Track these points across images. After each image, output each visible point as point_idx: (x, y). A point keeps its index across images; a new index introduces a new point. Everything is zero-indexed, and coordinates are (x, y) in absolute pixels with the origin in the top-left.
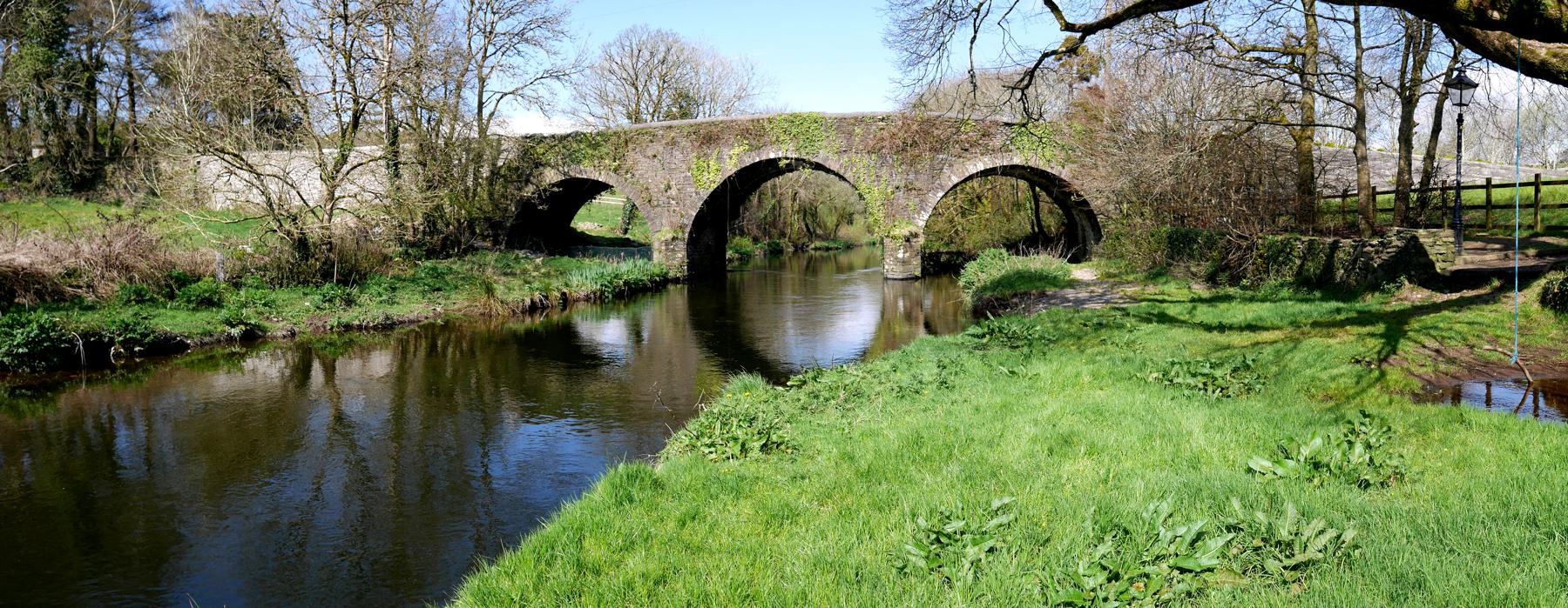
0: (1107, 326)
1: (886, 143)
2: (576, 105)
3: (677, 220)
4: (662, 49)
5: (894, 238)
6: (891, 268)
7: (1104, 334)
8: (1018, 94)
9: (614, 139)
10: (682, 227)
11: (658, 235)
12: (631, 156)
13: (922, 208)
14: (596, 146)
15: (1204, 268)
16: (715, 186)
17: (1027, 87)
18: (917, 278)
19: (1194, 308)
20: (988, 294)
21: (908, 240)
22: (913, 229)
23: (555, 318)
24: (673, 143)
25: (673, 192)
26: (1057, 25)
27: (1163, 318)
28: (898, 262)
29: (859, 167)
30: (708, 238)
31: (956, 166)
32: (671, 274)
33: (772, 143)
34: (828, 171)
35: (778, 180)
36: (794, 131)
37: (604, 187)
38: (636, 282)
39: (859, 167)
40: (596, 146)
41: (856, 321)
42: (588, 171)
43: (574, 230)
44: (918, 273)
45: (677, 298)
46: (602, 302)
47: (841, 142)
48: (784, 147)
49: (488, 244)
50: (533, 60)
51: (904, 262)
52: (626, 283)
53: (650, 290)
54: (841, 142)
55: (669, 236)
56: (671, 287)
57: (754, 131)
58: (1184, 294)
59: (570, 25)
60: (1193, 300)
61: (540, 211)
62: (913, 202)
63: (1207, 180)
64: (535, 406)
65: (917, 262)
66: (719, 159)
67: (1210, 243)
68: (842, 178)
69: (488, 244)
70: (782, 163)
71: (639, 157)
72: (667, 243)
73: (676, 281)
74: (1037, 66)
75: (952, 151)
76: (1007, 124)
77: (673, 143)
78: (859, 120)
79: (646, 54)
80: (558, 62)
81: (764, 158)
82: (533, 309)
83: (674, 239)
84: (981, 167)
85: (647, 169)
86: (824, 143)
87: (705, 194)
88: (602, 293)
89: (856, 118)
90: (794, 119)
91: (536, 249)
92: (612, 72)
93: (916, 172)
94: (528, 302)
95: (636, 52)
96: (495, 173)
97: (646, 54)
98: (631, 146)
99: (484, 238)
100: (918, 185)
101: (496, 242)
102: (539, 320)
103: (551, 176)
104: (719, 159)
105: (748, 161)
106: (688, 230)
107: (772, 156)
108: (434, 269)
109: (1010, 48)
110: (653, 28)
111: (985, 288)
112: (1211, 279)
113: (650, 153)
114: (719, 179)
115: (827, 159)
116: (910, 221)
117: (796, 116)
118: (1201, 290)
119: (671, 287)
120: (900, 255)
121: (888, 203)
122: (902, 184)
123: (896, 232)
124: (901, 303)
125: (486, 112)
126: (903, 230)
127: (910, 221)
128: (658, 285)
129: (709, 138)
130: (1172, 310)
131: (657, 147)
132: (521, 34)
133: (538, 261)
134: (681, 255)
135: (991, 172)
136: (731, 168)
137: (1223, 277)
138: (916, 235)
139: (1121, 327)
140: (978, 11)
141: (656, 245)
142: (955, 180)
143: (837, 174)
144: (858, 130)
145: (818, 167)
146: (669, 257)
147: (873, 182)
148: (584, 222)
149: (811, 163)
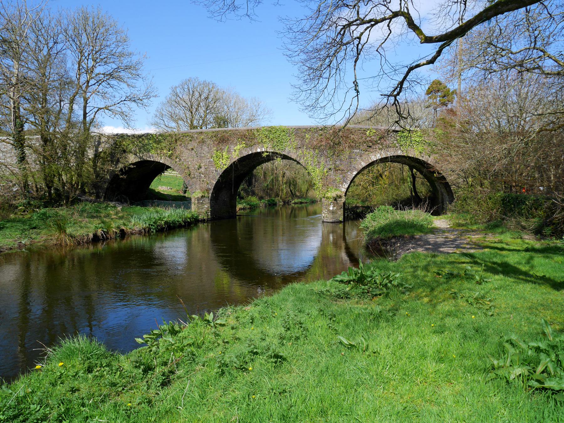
0: (458, 276)
1: (324, 143)
2: (157, 120)
3: (204, 186)
4: (206, 91)
5: (328, 198)
6: (325, 215)
7: (455, 284)
8: (392, 99)
9: (169, 138)
10: (208, 190)
11: (194, 195)
12: (179, 149)
13: (344, 181)
14: (159, 142)
15: (534, 222)
16: (226, 167)
17: (398, 94)
18: (340, 222)
19: (531, 258)
20: (376, 236)
21: (335, 200)
22: (339, 193)
23: (115, 245)
24: (203, 142)
25: (202, 170)
26: (417, 39)
27: (507, 270)
28: (329, 212)
29: (308, 158)
30: (224, 196)
31: (364, 157)
32: (200, 217)
33: (259, 143)
34: (290, 158)
35: (264, 165)
36: (271, 136)
37: (168, 167)
38: (174, 222)
39: (308, 158)
40: (159, 142)
41: (312, 245)
42: (154, 156)
43: (154, 190)
44: (341, 219)
45: (203, 233)
46: (150, 235)
47: (297, 143)
48: (266, 145)
49: (93, 198)
50: (119, 90)
51: (333, 212)
52: (166, 223)
53: (184, 227)
54: (297, 143)
55: (200, 195)
56: (201, 225)
57: (248, 137)
58: (517, 244)
59: (143, 72)
60: (527, 250)
61: (132, 179)
62: (338, 178)
63: (532, 161)
64: (120, 291)
65: (341, 212)
66: (229, 152)
67: (537, 205)
68: (298, 163)
69: (93, 198)
70: (265, 155)
71: (183, 149)
72: (198, 199)
73: (203, 221)
74: (405, 78)
75: (361, 147)
76: (394, 131)
77: (203, 142)
78: (308, 130)
79: (197, 94)
80: (135, 91)
81: (254, 151)
82: (96, 239)
83: (202, 197)
84: (378, 156)
85: (187, 156)
86: (289, 143)
87: (220, 172)
88: (150, 229)
89: (306, 129)
90: (271, 130)
91: (121, 201)
92: (178, 103)
93: (341, 160)
94: (91, 236)
95: (191, 92)
96: (97, 155)
97: (197, 94)
98: (179, 143)
99: (91, 194)
100: (342, 167)
101: (98, 197)
102: (101, 247)
103: (132, 159)
104: (229, 152)
105: (245, 153)
106: (211, 192)
107: (259, 150)
108: (44, 214)
109: (385, 67)
110: (201, 80)
111: (374, 232)
112: (538, 232)
113: (190, 147)
114: (228, 163)
115: (289, 152)
116: (337, 188)
117: (272, 128)
118: (531, 241)
119: (201, 225)
120: (331, 208)
121: (325, 178)
122: (332, 167)
123: (329, 195)
124: (331, 238)
125: (88, 119)
126: (332, 194)
127: (337, 188)
128: (190, 224)
129: (223, 140)
130: (512, 259)
131: (194, 144)
132: (111, 75)
133: (119, 208)
134: (207, 206)
135: (383, 160)
136: (235, 156)
137: (547, 231)
138: (340, 197)
139: (469, 277)
140: (359, 38)
141: (193, 200)
142: (364, 164)
143: (295, 161)
144: (307, 136)
145: (285, 157)
146: (200, 208)
147: (315, 167)
148: (160, 185)
149: (281, 155)
